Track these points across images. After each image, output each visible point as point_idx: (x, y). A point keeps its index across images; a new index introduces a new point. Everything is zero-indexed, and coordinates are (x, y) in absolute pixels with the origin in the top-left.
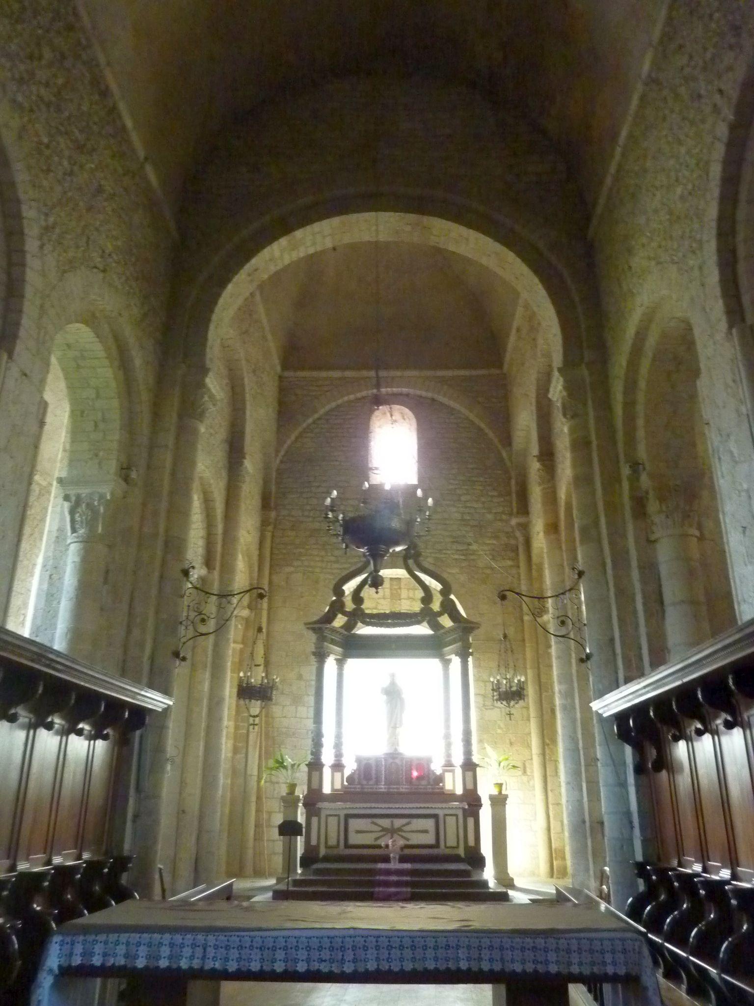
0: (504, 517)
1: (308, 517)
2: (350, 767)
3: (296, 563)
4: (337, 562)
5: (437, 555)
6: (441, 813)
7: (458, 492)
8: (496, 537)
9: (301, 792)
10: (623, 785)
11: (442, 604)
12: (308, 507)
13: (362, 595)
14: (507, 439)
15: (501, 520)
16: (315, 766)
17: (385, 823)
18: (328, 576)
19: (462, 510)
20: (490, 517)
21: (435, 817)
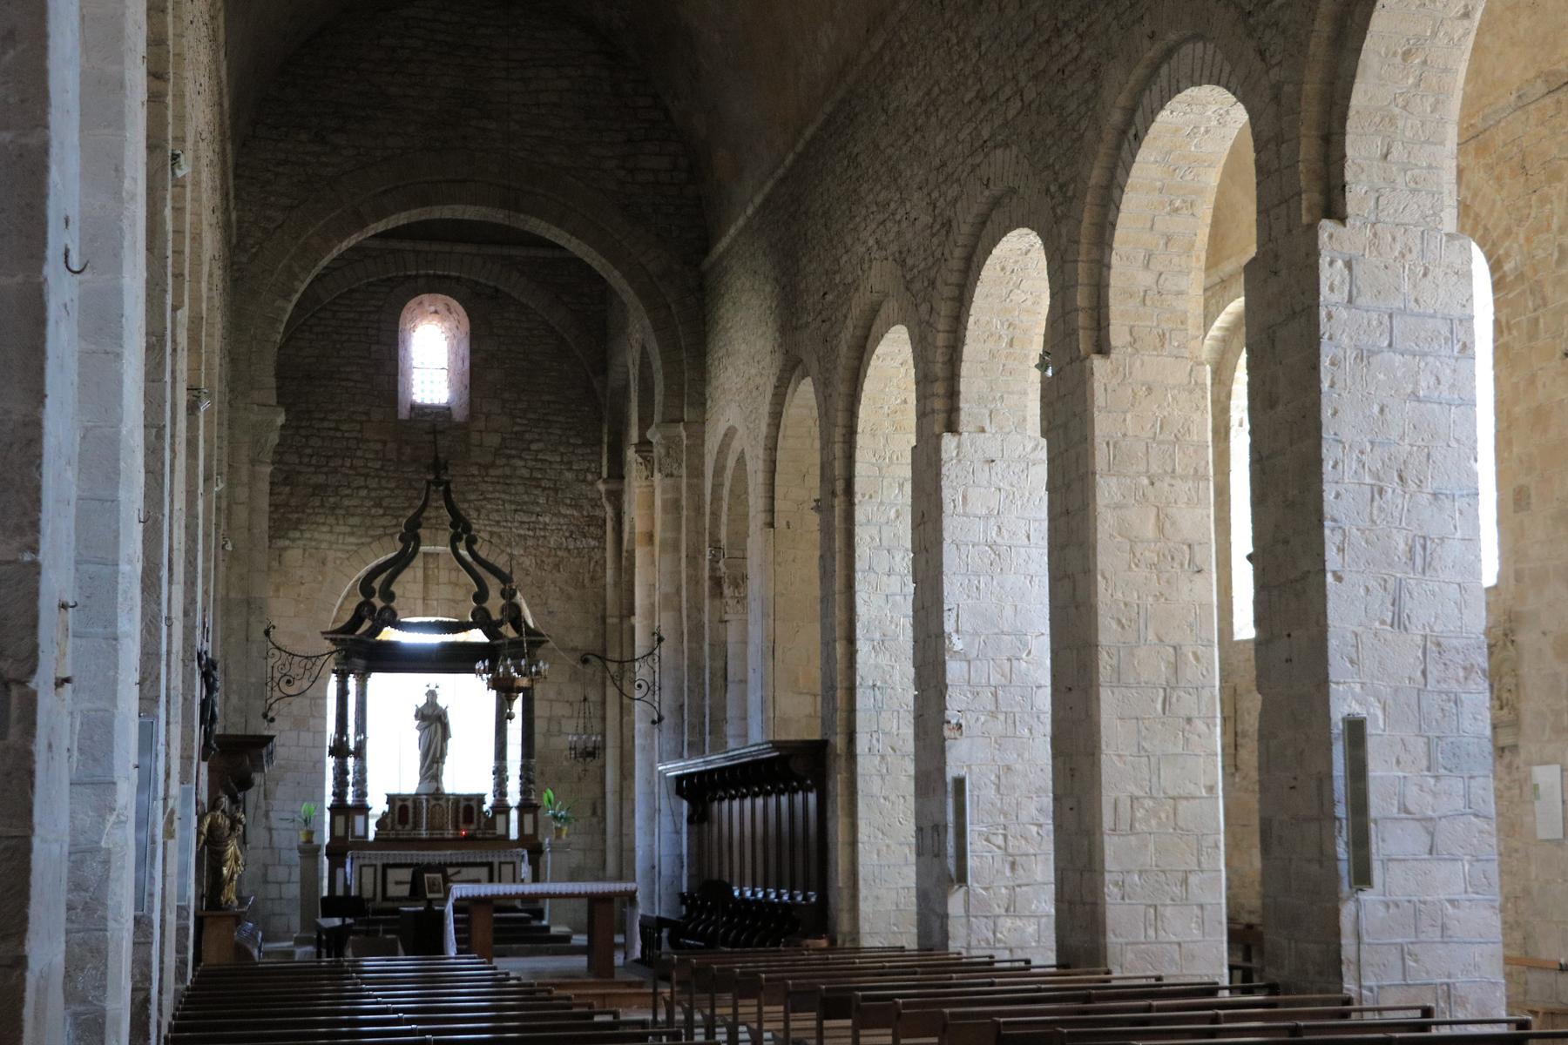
0: (589, 477)
1: (309, 465)
3: (291, 534)
4: (352, 534)
5: (495, 529)
6: (496, 861)
7: (527, 436)
8: (576, 506)
10: (678, 832)
11: (503, 610)
12: (309, 451)
13: (393, 588)
14: (602, 365)
15: (584, 481)
18: (339, 554)
19: (530, 464)
20: (569, 475)
21: (490, 865)
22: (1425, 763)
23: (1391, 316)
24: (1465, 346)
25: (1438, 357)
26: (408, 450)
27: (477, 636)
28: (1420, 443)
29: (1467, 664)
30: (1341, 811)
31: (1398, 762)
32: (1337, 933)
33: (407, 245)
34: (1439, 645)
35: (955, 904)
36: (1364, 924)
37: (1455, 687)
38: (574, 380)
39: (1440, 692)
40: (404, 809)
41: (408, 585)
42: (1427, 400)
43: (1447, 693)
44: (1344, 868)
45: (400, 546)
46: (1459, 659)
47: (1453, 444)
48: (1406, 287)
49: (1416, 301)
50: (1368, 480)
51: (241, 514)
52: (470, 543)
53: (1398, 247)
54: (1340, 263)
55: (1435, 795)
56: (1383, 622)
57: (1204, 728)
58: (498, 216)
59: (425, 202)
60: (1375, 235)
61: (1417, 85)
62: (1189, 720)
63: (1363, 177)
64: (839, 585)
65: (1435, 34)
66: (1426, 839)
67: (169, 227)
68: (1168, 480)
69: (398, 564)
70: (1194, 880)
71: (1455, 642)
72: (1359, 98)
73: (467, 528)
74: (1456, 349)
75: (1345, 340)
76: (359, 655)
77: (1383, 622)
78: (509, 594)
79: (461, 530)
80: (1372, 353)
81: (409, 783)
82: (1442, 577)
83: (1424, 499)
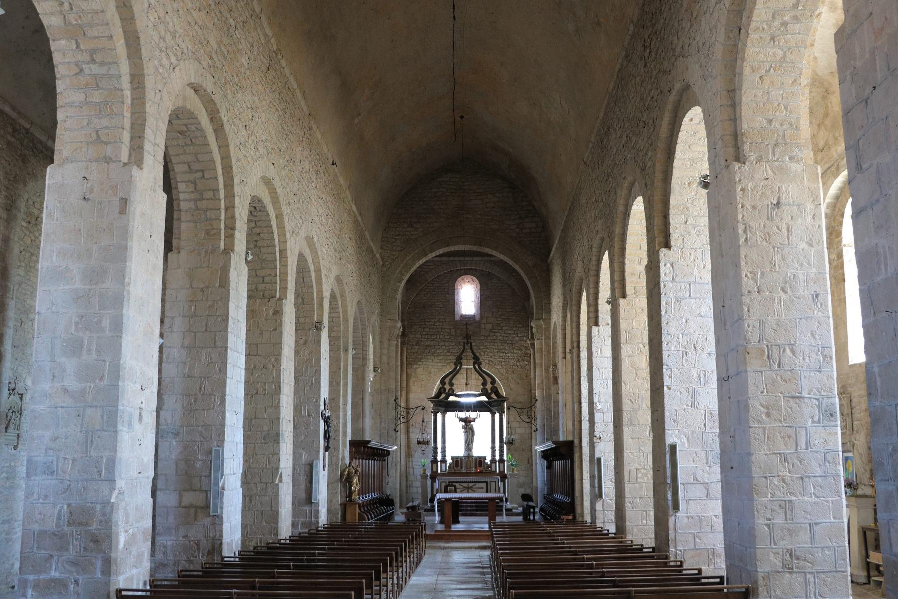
2: (449, 461)
8: (521, 350)
9: (428, 473)
11: (492, 389)
16: (434, 461)
17: (466, 485)
20: (517, 339)
21: (487, 482)
26: (459, 331)
27: (484, 398)
30: (669, 481)
32: (667, 529)
33: (456, 258)
35: (599, 506)
36: (678, 525)
38: (518, 304)
40: (457, 461)
41: (460, 380)
44: (670, 503)
45: (454, 367)
48: (696, 272)
50: (681, 349)
51: (385, 358)
52: (480, 364)
53: (692, 257)
54: (668, 265)
55: (709, 474)
58: (475, 248)
59: (448, 245)
64: (575, 382)
66: (705, 491)
67: (312, 268)
69: (455, 373)
72: (673, 201)
73: (479, 359)
75: (671, 294)
76: (440, 406)
78: (494, 382)
79: (477, 361)
80: (682, 299)
81: (461, 452)
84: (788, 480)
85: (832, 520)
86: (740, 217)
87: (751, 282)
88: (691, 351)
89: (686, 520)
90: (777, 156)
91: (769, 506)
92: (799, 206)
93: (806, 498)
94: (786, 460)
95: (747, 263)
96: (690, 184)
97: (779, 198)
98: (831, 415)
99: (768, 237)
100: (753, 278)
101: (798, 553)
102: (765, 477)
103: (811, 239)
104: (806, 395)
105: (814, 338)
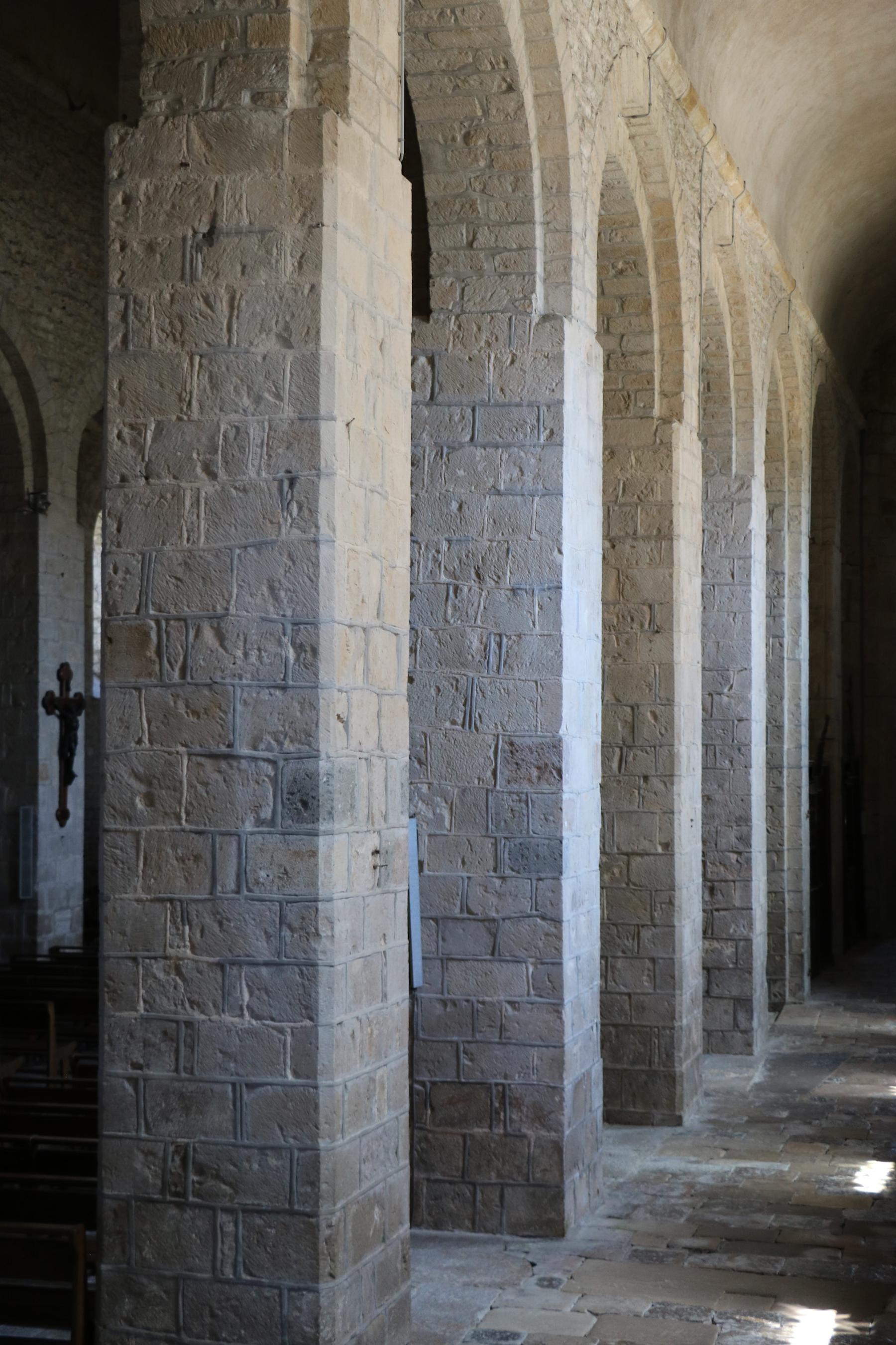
22: (491, 863)
23: (474, 410)
24: (552, 432)
25: (522, 446)
28: (499, 537)
29: (541, 763)
31: (463, 863)
34: (512, 744)
37: (526, 787)
39: (510, 793)
42: (509, 492)
43: (518, 794)
46: (532, 758)
47: (534, 535)
48: (491, 376)
49: (502, 390)
50: (443, 578)
55: (500, 896)
56: (454, 723)
57: (662, 786)
60: (459, 327)
61: (491, 165)
62: (646, 778)
63: (449, 269)
65: (486, 112)
66: (488, 940)
68: (629, 541)
70: (646, 934)
71: (529, 741)
74: (543, 438)
77: (454, 723)
80: (452, 449)
82: (517, 675)
83: (502, 596)
84: (188, 968)
85: (290, 1077)
86: (114, 278)
87: (130, 452)
88: (469, 585)
89: (439, 1009)
90: (219, 95)
91: (139, 1034)
92: (263, 233)
93: (228, 1018)
94: (186, 918)
95: (122, 403)
96: (467, 137)
97: (214, 217)
98: (305, 804)
99: (178, 330)
100: (134, 442)
101: (201, 1158)
102: (135, 959)
103: (287, 328)
104: (245, 751)
105: (276, 598)
